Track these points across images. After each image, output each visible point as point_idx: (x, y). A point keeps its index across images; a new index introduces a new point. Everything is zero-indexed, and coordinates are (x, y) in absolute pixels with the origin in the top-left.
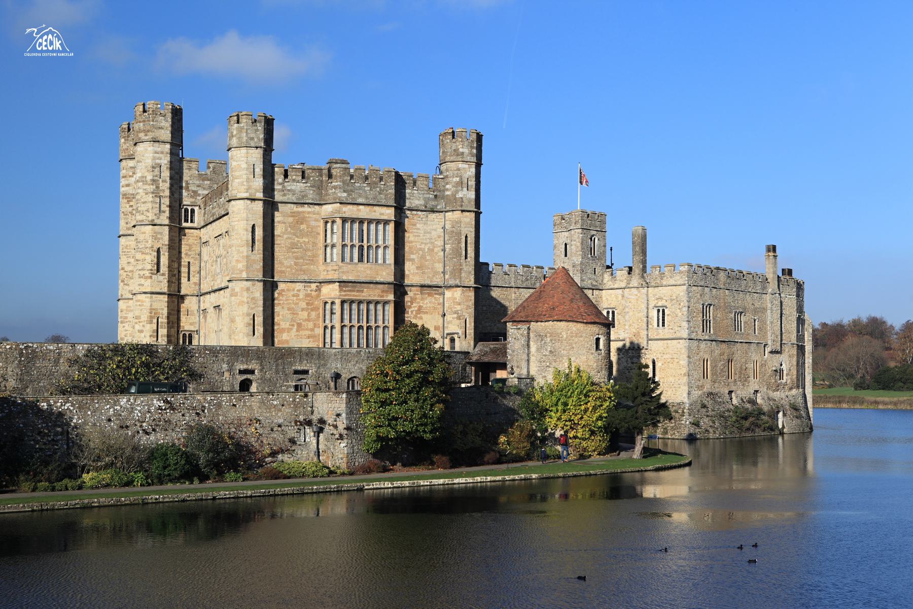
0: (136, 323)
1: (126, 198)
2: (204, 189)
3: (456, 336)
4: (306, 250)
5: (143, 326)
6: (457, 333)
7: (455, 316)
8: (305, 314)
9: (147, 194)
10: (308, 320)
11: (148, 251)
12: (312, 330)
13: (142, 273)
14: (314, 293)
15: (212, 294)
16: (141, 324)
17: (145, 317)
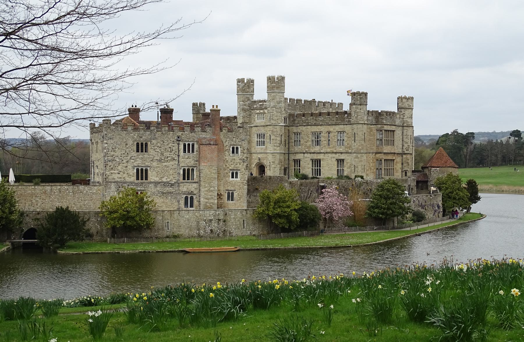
0: (273, 164)
1: (244, 110)
2: (289, 110)
3: (407, 171)
4: (372, 141)
5: (276, 166)
6: (408, 170)
7: (407, 164)
8: (372, 164)
9: (277, 112)
10: (372, 166)
11: (278, 136)
12: (373, 170)
13: (275, 144)
14: (374, 157)
15: (309, 154)
16: (275, 165)
17: (277, 162)
